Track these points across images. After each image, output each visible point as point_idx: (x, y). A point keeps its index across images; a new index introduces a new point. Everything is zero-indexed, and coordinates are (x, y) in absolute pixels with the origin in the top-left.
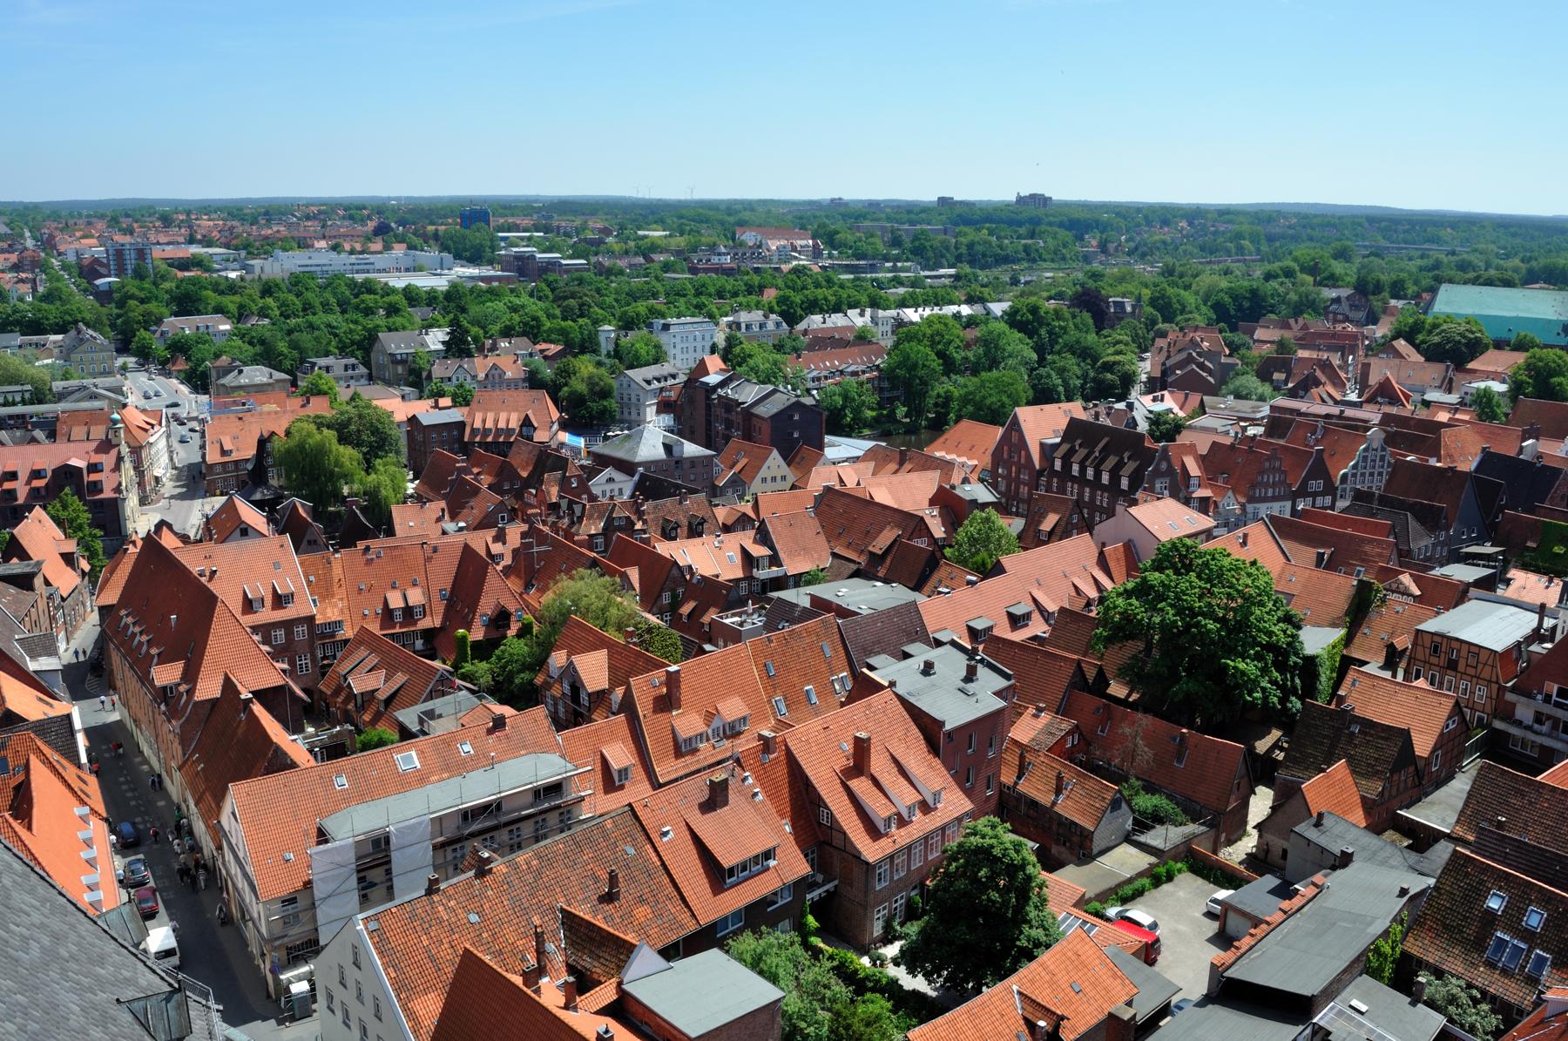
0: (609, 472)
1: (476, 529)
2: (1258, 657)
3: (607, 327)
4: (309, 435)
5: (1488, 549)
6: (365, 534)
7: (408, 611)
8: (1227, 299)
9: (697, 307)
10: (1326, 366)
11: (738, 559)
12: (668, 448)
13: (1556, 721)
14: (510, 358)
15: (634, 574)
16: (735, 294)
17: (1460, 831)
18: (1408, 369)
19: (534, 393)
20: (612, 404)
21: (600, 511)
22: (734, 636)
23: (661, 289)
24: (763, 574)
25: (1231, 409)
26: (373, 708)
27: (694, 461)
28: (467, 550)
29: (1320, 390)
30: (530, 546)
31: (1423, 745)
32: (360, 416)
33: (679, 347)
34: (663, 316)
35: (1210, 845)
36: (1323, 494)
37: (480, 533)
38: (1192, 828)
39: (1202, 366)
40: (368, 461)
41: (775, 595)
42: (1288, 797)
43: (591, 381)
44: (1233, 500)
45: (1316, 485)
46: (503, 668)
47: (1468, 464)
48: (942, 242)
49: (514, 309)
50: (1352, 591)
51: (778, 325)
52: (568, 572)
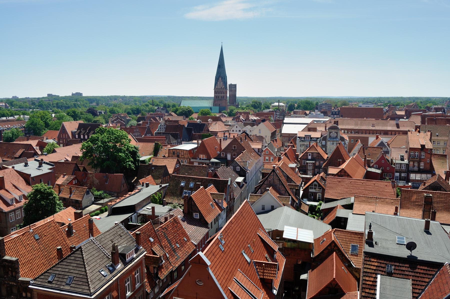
39: (120, 119)
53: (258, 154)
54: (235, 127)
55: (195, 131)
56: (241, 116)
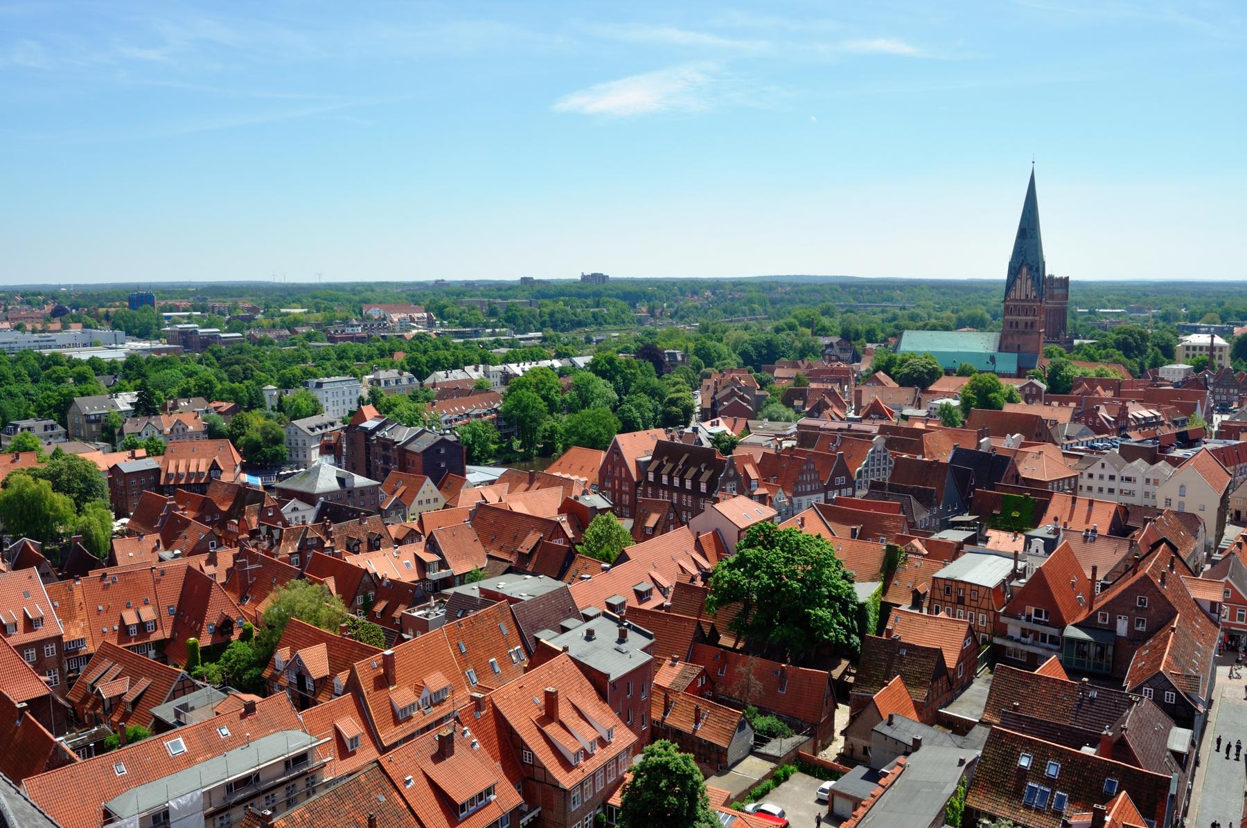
0: (293, 503)
1: (189, 555)
2: (830, 606)
3: (270, 387)
4: (26, 485)
5: (966, 517)
6: (95, 565)
7: (142, 626)
8: (750, 348)
9: (341, 368)
10: (831, 393)
11: (413, 566)
12: (341, 481)
13: (1036, 633)
14: (191, 414)
15: (331, 582)
16: (370, 357)
17: (987, 717)
18: (888, 392)
19: (219, 442)
20: (283, 448)
21: (295, 534)
22: (422, 626)
23: (309, 355)
24: (434, 575)
25: (768, 429)
26: (121, 709)
27: (363, 490)
28: (190, 569)
29: (829, 411)
30: (244, 564)
31: (951, 660)
32: (70, 467)
33: (330, 400)
34: (315, 376)
35: (811, 750)
36: (846, 486)
37: (195, 558)
38: (797, 739)
39: (742, 398)
40: (78, 505)
41: (450, 591)
42: (861, 707)
43: (264, 431)
44: (783, 495)
45: (840, 480)
46: (232, 668)
47: (946, 458)
48: (529, 312)
49: (191, 374)
50: (884, 554)
51: (410, 380)
52: (282, 583)
53: (1212, 621)
54: (1099, 464)
55: (988, 493)
56: (1102, 407)
